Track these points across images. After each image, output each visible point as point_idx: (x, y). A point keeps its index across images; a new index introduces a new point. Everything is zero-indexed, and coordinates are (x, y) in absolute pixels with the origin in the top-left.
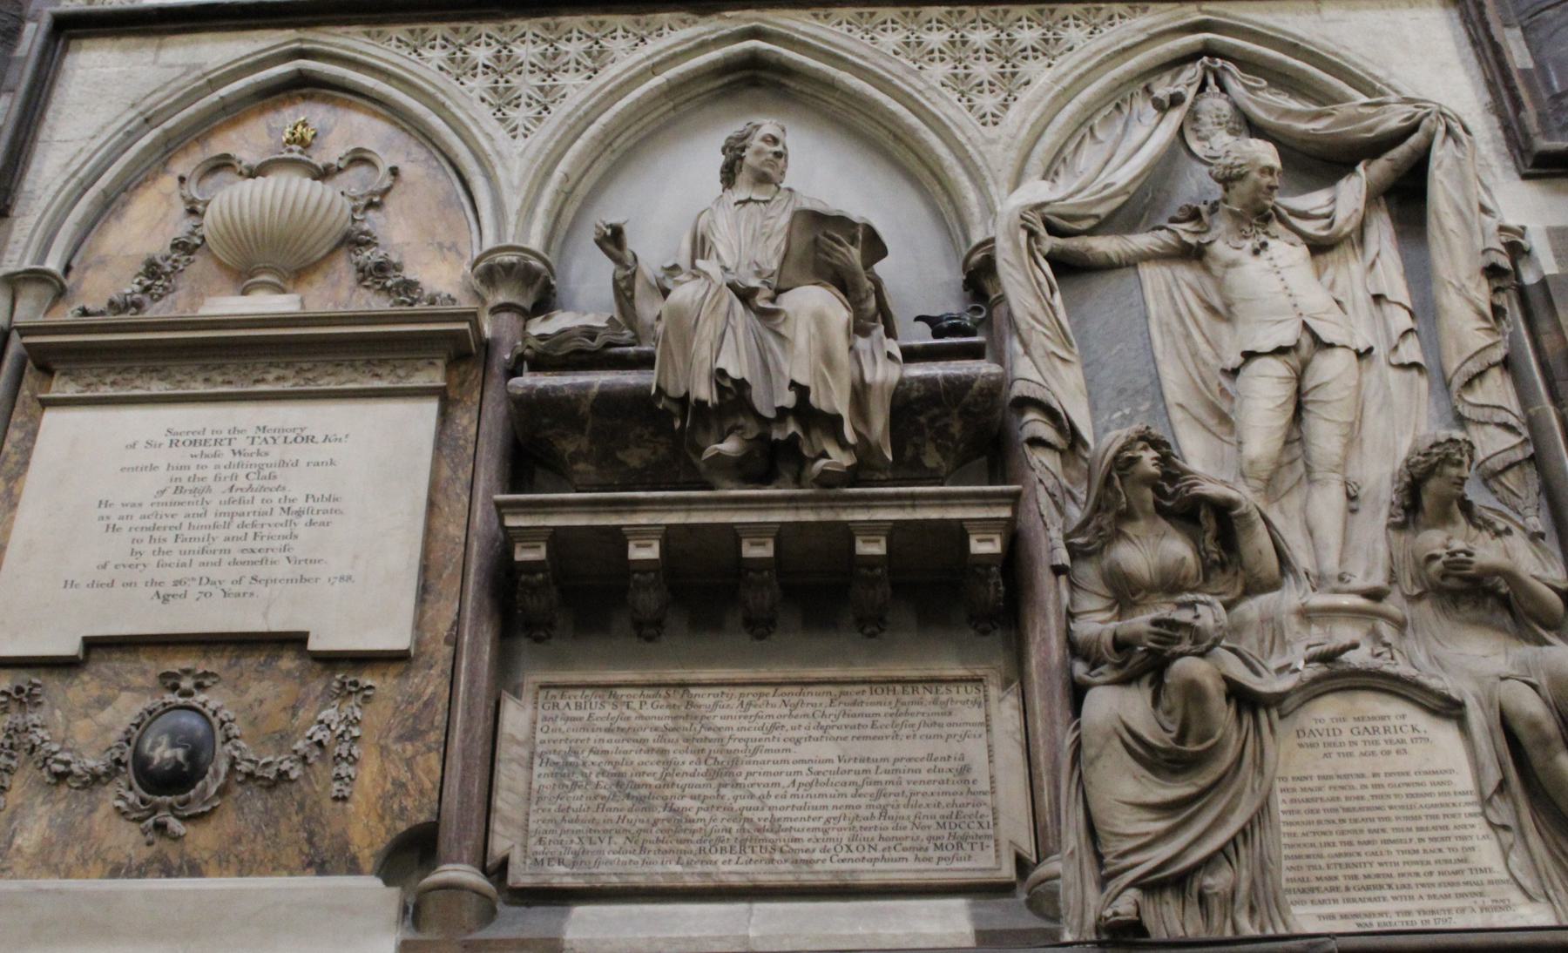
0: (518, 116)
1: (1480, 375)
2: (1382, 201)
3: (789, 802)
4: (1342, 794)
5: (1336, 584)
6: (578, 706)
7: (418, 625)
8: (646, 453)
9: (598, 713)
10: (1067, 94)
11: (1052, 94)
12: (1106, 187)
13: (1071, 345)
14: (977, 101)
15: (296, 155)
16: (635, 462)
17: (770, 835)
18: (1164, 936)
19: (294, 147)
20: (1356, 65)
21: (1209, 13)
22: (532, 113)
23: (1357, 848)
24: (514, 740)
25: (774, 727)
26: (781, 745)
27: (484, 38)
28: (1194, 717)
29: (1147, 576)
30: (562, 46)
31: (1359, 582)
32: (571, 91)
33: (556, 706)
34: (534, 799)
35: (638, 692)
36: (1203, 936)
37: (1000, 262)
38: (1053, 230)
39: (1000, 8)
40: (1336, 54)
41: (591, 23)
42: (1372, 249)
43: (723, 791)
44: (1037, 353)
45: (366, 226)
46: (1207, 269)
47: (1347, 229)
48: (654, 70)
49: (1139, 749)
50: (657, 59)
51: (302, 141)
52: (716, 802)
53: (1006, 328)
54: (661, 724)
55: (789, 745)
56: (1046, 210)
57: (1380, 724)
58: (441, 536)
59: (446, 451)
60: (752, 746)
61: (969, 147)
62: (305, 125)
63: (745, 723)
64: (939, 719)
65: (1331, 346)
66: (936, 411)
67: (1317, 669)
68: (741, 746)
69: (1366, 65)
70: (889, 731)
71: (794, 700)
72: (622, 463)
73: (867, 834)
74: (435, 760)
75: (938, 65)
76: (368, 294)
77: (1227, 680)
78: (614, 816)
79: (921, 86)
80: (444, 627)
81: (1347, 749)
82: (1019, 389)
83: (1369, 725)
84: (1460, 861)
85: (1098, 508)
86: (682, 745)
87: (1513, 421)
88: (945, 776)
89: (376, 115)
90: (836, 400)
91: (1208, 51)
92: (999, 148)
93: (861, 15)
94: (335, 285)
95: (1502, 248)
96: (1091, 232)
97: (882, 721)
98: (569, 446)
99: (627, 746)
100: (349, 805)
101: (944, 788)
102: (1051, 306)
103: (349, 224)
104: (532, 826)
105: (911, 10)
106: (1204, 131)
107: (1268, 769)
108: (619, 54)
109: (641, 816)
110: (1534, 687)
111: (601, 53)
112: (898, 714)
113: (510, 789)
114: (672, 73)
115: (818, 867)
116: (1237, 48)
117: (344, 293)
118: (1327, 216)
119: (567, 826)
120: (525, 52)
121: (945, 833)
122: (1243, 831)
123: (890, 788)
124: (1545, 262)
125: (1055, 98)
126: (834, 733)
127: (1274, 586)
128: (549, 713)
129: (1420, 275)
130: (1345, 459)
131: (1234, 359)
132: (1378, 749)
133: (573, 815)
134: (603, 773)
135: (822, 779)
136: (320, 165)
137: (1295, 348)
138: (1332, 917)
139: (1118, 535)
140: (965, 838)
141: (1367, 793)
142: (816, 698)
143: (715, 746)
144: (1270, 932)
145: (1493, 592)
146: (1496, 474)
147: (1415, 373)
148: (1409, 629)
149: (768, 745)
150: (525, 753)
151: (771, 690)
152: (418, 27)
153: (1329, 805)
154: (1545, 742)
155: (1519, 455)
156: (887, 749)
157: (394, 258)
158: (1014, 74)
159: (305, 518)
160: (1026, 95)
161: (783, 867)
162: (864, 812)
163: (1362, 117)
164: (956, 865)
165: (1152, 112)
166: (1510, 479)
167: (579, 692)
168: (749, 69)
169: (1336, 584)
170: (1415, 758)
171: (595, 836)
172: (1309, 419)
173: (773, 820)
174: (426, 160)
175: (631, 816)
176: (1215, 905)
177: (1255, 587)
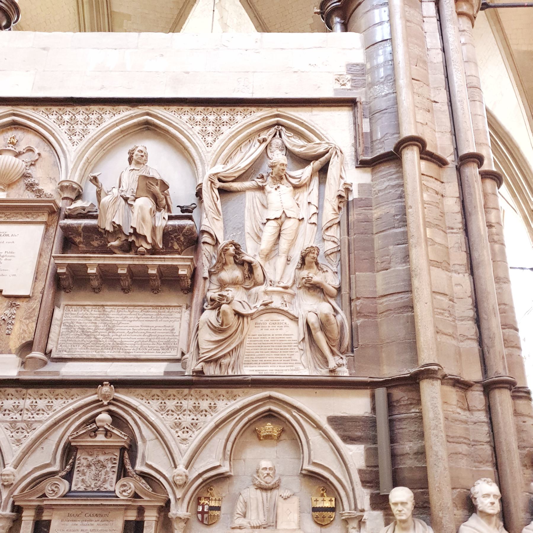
0: (75, 138)
1: (331, 227)
2: (317, 173)
3: (126, 337)
4: (263, 339)
5: (277, 284)
6: (75, 311)
7: (34, 288)
8: (99, 242)
9: (80, 313)
10: (234, 137)
11: (229, 137)
12: (238, 168)
13: (220, 215)
14: (207, 139)
15: (10, 148)
16: (96, 245)
17: (120, 346)
18: (208, 374)
19: (10, 145)
20: (318, 130)
21: (280, 111)
22: (79, 138)
23: (264, 353)
24: (57, 319)
25: (125, 317)
26: (127, 322)
27: (68, 112)
28: (225, 320)
29: (228, 281)
30: (91, 116)
31: (282, 285)
32: (91, 131)
33: (69, 310)
34: (61, 334)
35: (91, 307)
36: (219, 374)
37: (203, 191)
38: (220, 180)
39: (219, 108)
40: (313, 126)
41: (100, 109)
42: (311, 188)
43: (110, 334)
44: (209, 218)
45: (29, 171)
46: (264, 193)
47: (304, 182)
48: (117, 125)
49: (212, 327)
50: (117, 121)
51: (12, 143)
52: (107, 337)
53: (203, 210)
54: (96, 316)
55: (129, 322)
56: (219, 175)
57: (277, 322)
58: (42, 264)
59: (46, 240)
60: (119, 322)
61: (202, 154)
62: (13, 138)
63: (118, 316)
64: (169, 316)
65: (290, 218)
66: (176, 234)
67: (263, 307)
68: (116, 322)
69: (321, 130)
70: (155, 319)
71: (132, 310)
72: (91, 245)
73: (145, 346)
74: (34, 325)
75: (198, 126)
76: (29, 192)
77: (234, 310)
78: (81, 339)
79: (192, 133)
80: (40, 289)
81: (267, 328)
82: (203, 228)
83: (274, 322)
84: (291, 358)
85: (218, 262)
86: (101, 321)
87: (336, 240)
88: (167, 331)
89: (36, 135)
90: (146, 232)
91: (278, 124)
92: (210, 154)
93: (178, 109)
94: (20, 189)
95: (344, 190)
96: (233, 181)
97: (154, 316)
98: (78, 240)
99: (86, 321)
100: (11, 336)
101: (167, 334)
102: (215, 204)
103: (25, 170)
104: (59, 342)
105: (193, 108)
106: (272, 150)
107: (244, 333)
108: (107, 120)
109: (88, 340)
110: (317, 314)
111: (101, 119)
112: (158, 315)
113: (54, 332)
114: (121, 126)
115: (131, 354)
116: (286, 123)
117: (21, 192)
118: (300, 178)
119: (69, 342)
120: (80, 118)
121: (165, 346)
122: (235, 348)
123: (153, 334)
124: (354, 195)
125: (230, 138)
126: (141, 319)
127: (262, 284)
128: (67, 312)
129: (321, 196)
130: (289, 250)
131: (265, 221)
132: (275, 328)
133: (70, 339)
134: (79, 328)
135: (136, 331)
136: (17, 152)
137: (280, 218)
138: (253, 370)
139: (222, 269)
140: (170, 347)
141: (269, 340)
142: (138, 310)
143: (109, 322)
144: (236, 374)
145: (319, 287)
146: (328, 255)
147: (314, 225)
148: (296, 297)
149: (123, 322)
150: (59, 323)
151: (126, 308)
152: (49, 107)
153: (259, 342)
154: (315, 329)
155: (336, 250)
156: (154, 324)
157: (36, 182)
158: (219, 130)
159: (5, 258)
160: (221, 137)
161: (122, 354)
162: (145, 340)
163: (314, 148)
164: (167, 354)
165: (258, 144)
166: (332, 257)
167: (75, 307)
168: (146, 125)
169: (277, 284)
170: (284, 331)
171: (75, 345)
172: (281, 238)
173: (121, 342)
174: (49, 151)
175: (85, 340)
176: (223, 367)
177: (256, 284)
